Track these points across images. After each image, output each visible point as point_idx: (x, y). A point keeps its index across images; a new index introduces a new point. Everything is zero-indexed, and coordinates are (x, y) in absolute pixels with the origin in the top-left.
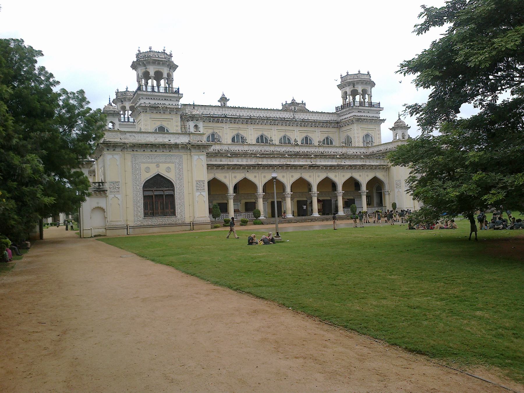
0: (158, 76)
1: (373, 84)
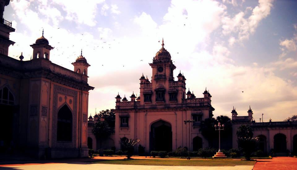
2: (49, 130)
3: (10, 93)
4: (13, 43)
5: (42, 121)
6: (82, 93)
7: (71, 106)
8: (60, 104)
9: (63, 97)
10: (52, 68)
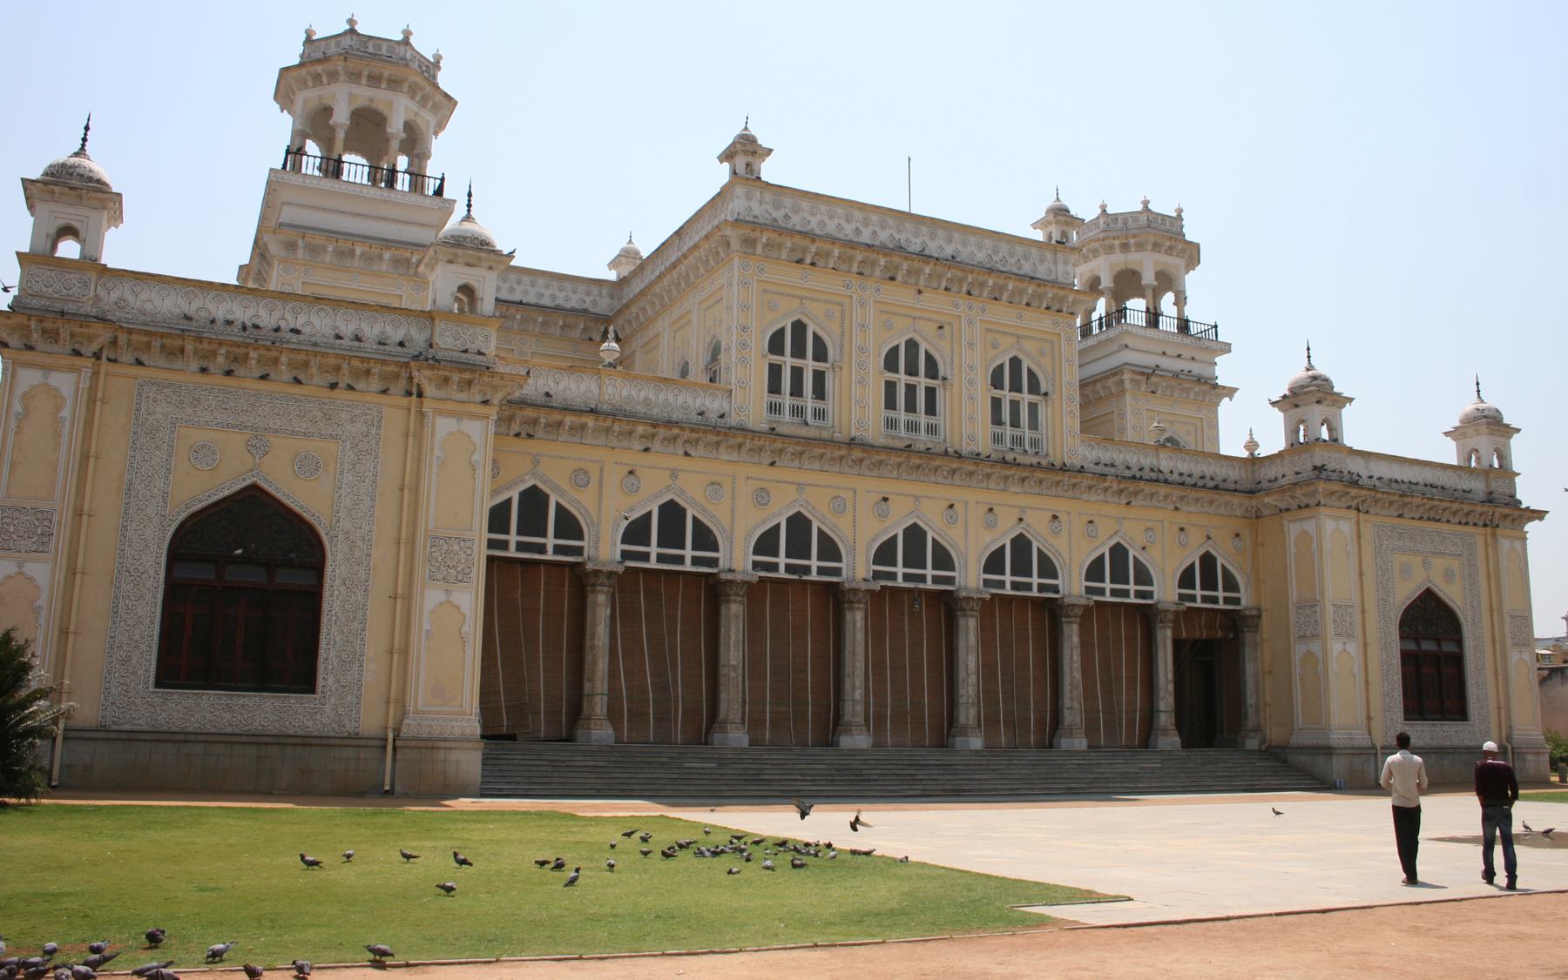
0: (368, 131)
1: (1192, 255)
2: (1367, 683)
3: (1223, 567)
4: (1230, 392)
5: (1335, 654)
6: (1494, 535)
7: (1452, 594)
8: (1405, 592)
9: (1416, 561)
10: (1357, 466)
